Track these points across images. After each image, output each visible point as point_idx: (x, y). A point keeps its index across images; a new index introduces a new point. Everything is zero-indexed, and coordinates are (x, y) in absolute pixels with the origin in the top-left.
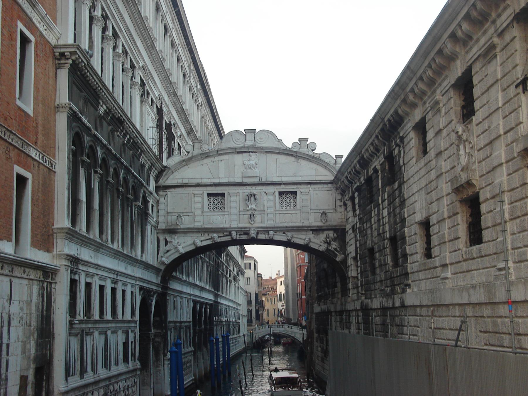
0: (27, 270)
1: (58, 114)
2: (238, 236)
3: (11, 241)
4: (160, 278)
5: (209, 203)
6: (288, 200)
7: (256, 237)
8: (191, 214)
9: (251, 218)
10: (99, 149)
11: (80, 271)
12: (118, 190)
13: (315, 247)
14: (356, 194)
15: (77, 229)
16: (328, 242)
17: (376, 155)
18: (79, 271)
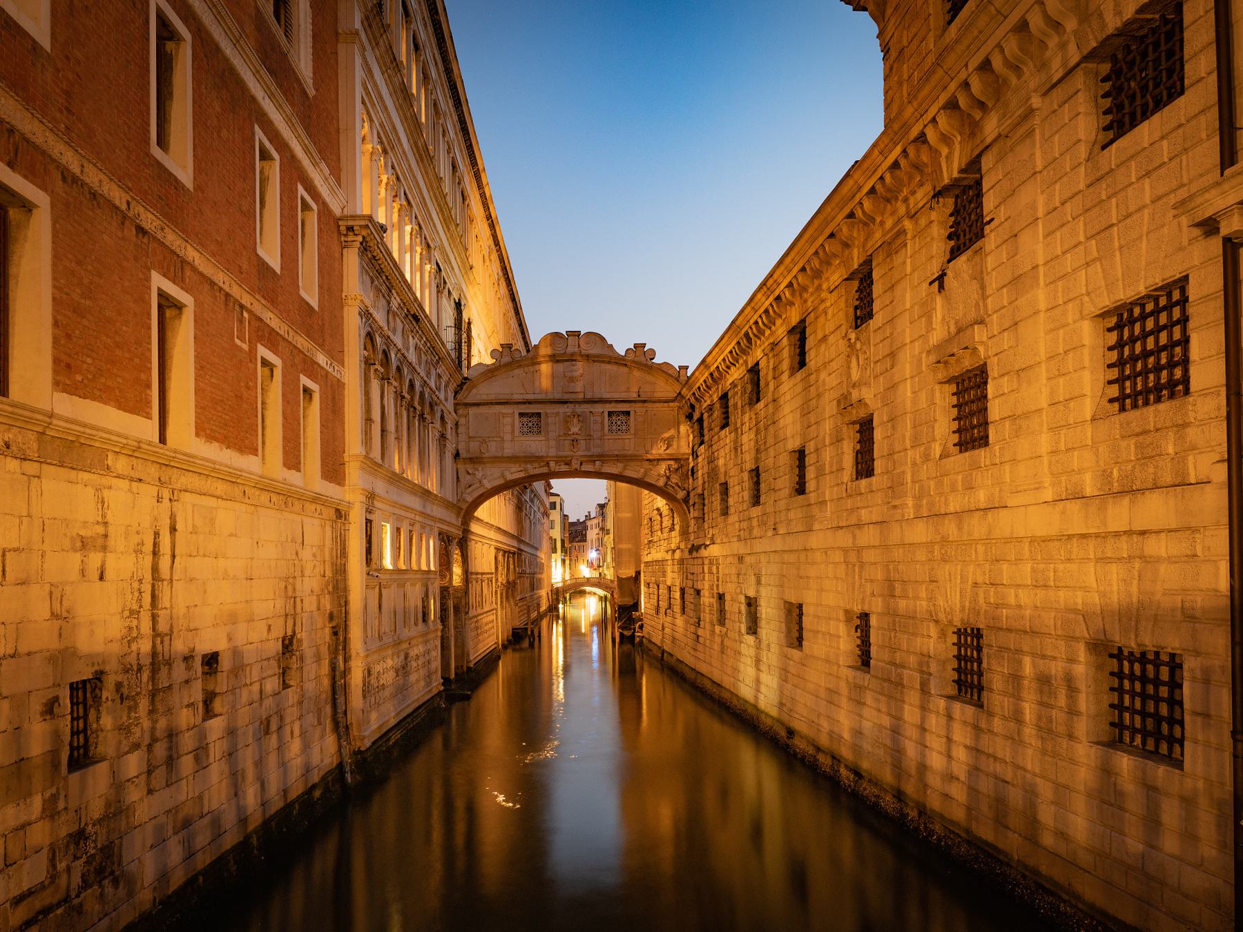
0: (319, 507)
1: (346, 308)
2: (558, 467)
3: (300, 471)
4: (460, 519)
6: (619, 423)
8: (499, 439)
10: (393, 356)
11: (374, 509)
12: (415, 408)
14: (706, 416)
15: (371, 456)
17: (735, 365)
18: (374, 509)
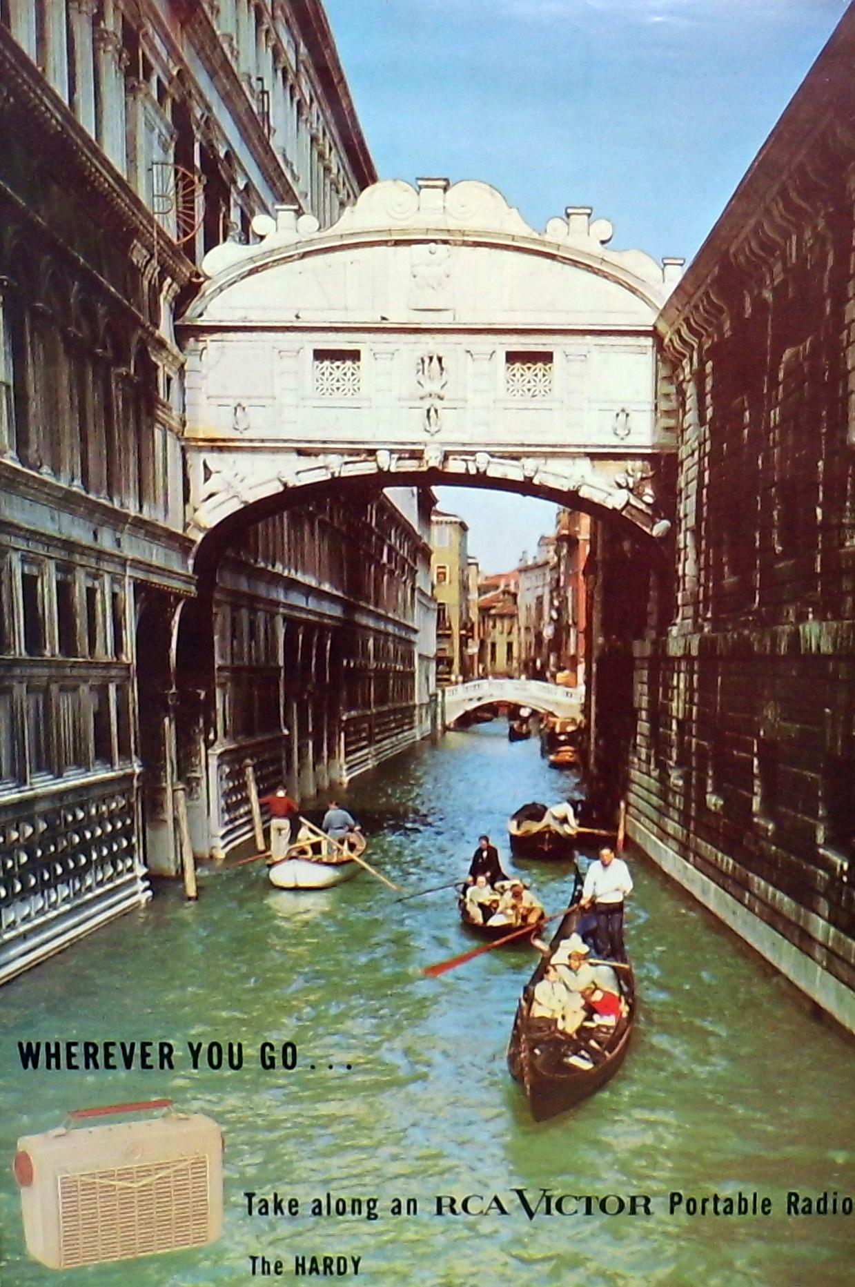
2: (394, 462)
5: (318, 374)
7: (440, 468)
9: (428, 417)
13: (597, 497)
16: (631, 485)
